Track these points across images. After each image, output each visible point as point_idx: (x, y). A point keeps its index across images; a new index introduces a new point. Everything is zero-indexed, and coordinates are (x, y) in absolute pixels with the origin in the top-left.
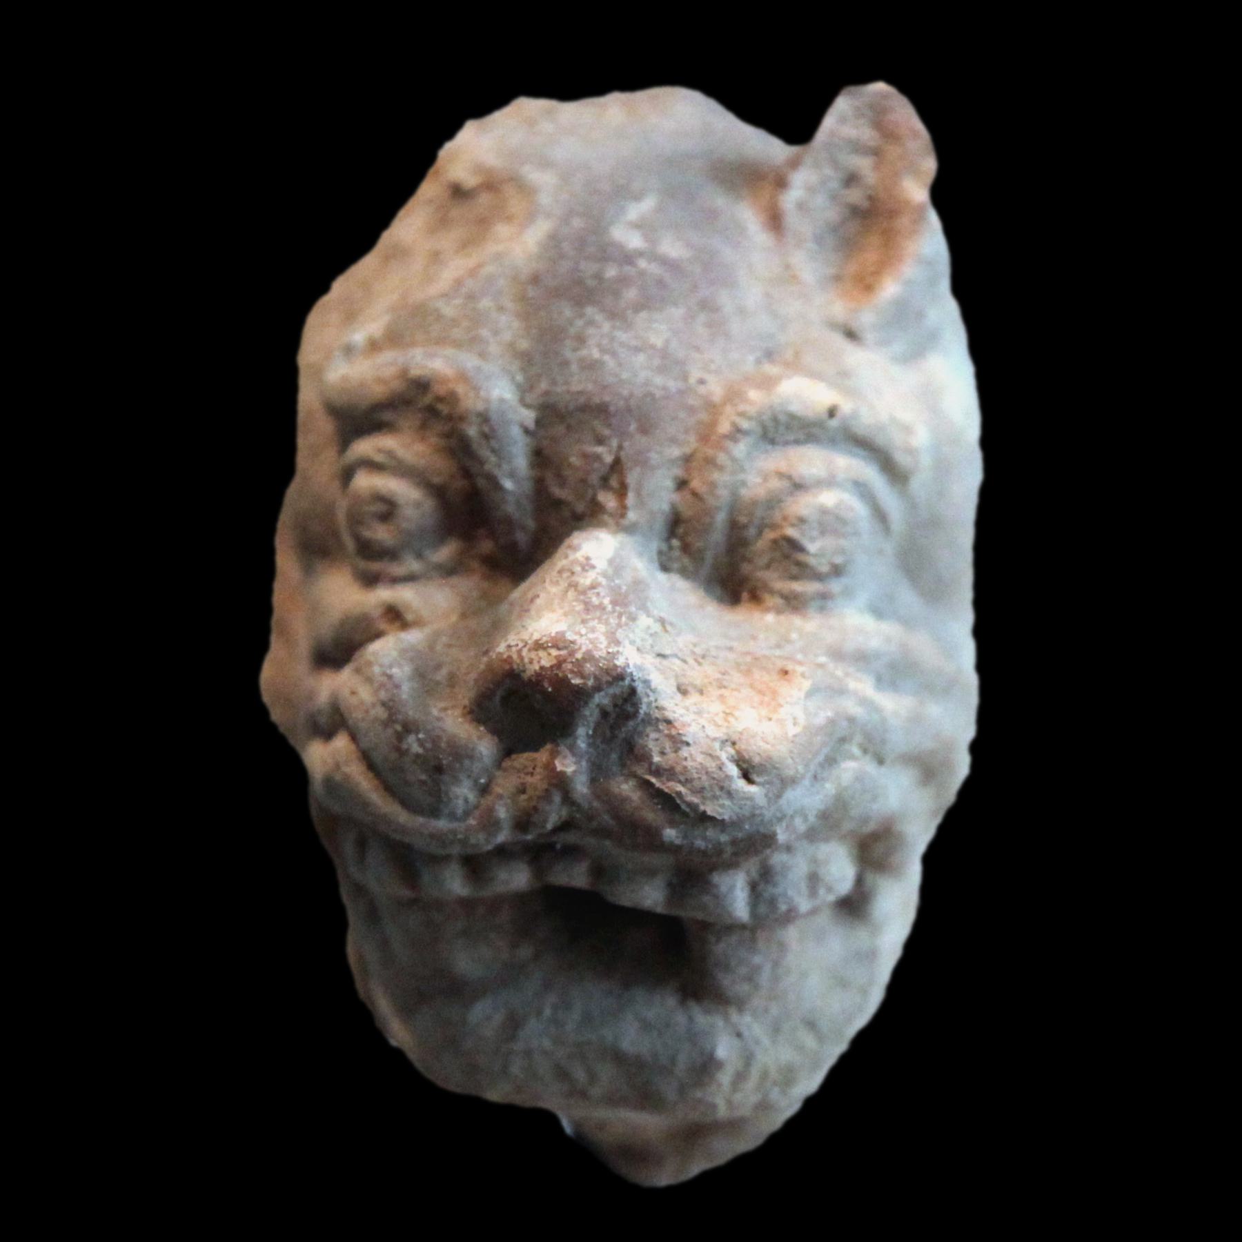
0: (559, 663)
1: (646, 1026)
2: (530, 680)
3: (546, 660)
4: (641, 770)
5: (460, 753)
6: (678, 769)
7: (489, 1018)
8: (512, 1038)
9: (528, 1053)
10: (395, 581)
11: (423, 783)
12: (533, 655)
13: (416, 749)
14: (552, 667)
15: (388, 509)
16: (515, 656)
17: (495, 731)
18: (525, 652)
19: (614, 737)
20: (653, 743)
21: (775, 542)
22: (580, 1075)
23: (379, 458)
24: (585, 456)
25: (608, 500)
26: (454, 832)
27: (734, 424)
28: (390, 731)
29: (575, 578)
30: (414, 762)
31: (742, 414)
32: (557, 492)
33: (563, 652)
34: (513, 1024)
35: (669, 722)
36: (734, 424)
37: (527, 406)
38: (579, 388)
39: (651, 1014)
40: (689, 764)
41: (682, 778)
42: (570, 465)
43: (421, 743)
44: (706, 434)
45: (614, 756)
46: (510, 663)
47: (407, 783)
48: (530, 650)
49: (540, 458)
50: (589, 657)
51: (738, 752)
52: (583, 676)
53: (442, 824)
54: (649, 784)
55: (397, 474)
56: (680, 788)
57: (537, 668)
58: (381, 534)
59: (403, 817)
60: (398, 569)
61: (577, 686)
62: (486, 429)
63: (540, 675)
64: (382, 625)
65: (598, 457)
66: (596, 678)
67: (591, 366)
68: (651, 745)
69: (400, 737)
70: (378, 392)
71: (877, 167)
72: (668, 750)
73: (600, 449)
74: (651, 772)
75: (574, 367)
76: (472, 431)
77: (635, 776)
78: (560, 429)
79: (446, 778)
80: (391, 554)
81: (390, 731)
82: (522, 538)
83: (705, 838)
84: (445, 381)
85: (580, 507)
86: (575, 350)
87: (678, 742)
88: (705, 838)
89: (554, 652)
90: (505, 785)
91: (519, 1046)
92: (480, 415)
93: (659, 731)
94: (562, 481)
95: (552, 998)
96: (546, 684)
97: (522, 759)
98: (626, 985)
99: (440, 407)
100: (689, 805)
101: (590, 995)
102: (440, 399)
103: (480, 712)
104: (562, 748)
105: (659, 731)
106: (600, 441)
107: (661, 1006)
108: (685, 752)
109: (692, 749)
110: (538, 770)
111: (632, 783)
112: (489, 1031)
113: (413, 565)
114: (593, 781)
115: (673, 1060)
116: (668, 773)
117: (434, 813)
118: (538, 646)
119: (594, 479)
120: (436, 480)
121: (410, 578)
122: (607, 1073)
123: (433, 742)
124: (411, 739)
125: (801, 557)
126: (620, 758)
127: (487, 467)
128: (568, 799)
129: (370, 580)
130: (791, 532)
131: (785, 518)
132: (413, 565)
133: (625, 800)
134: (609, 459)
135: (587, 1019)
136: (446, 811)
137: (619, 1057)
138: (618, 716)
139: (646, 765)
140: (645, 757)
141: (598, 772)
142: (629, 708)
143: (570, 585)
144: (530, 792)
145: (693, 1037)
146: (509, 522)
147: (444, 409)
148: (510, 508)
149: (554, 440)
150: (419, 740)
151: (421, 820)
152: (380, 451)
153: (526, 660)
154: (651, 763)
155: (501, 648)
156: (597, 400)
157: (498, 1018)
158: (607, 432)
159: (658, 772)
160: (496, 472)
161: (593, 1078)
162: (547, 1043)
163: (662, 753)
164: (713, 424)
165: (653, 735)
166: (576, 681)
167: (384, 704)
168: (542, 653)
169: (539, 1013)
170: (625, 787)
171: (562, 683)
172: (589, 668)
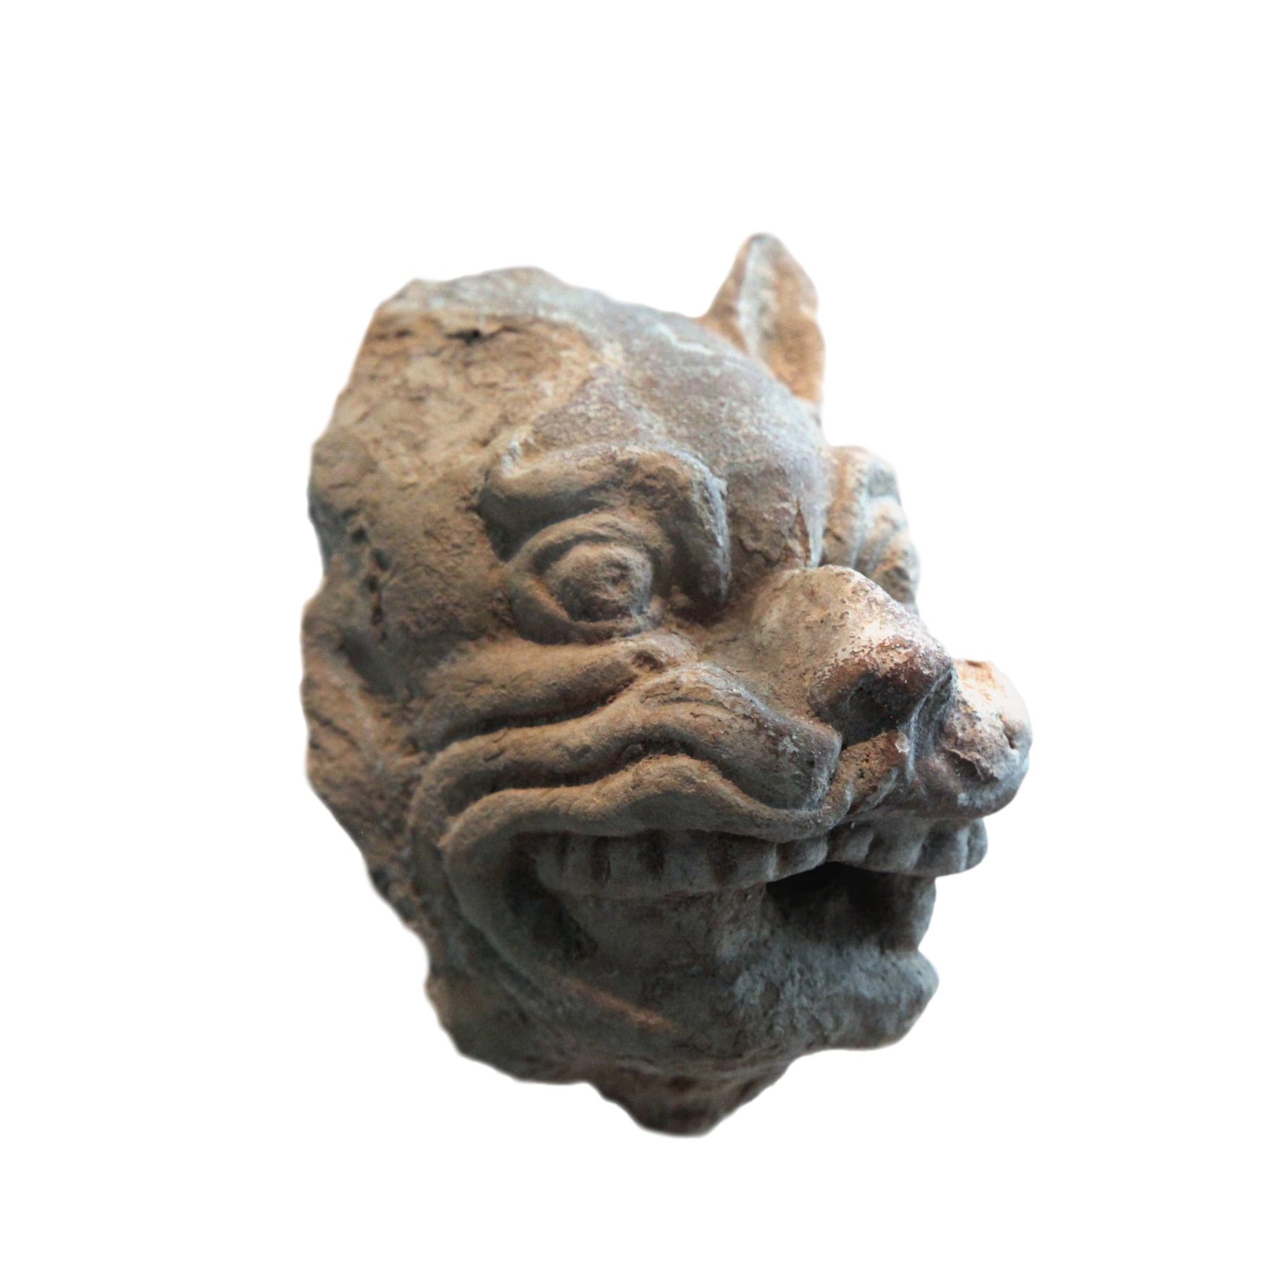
0: (911, 660)
1: (870, 974)
2: (885, 677)
3: (898, 658)
4: (947, 745)
5: (825, 749)
6: (977, 740)
7: (752, 990)
8: (777, 1000)
9: (791, 1012)
10: (625, 634)
11: (799, 777)
12: (883, 656)
13: (792, 748)
14: (905, 663)
15: (622, 572)
16: (867, 660)
17: (838, 728)
18: (874, 654)
19: (931, 719)
20: (956, 721)
21: (887, 573)
22: (829, 1023)
23: (602, 532)
24: (776, 511)
25: (798, 549)
26: (814, 818)
27: (858, 480)
28: (762, 738)
29: (870, 595)
30: (791, 760)
31: (860, 471)
32: (751, 544)
33: (910, 650)
34: (774, 991)
35: (964, 703)
36: (858, 480)
37: (720, 477)
38: (758, 457)
39: (870, 965)
40: (983, 735)
41: (979, 747)
42: (764, 520)
43: (795, 743)
44: (839, 488)
45: (930, 736)
46: (866, 666)
47: (782, 781)
48: (878, 653)
49: (735, 518)
50: (928, 653)
51: (1005, 723)
52: (930, 668)
53: (804, 812)
54: (955, 756)
55: (615, 544)
56: (978, 756)
57: (892, 665)
58: (614, 594)
59: (766, 811)
60: (625, 624)
61: (928, 676)
62: (707, 495)
63: (895, 672)
64: (635, 670)
65: (786, 512)
66: (938, 669)
67: (756, 440)
68: (956, 723)
69: (775, 741)
70: (590, 478)
71: (779, 299)
72: (968, 727)
73: (786, 505)
74: (956, 745)
75: (743, 441)
76: (696, 498)
77: (944, 751)
78: (746, 493)
79: (815, 770)
80: (623, 612)
81: (762, 738)
82: (724, 586)
83: (982, 798)
84: (654, 461)
85: (775, 554)
86: (735, 430)
87: (972, 718)
88: (982, 798)
89: (903, 651)
90: (849, 773)
91: (782, 1008)
92: (700, 483)
93: (959, 711)
94: (757, 535)
95: (796, 964)
96: (902, 678)
97: (859, 749)
98: (839, 947)
99: (649, 482)
100: (983, 770)
101: (820, 956)
102: (649, 476)
103: (825, 712)
104: (900, 733)
105: (959, 711)
106: (784, 498)
107: (868, 957)
108: (979, 726)
109: (983, 722)
110: (872, 755)
111: (942, 756)
112: (755, 1001)
113: (639, 620)
114: (917, 758)
115: (899, 999)
116: (971, 745)
117: (797, 804)
118: (883, 648)
119: (784, 529)
120: (653, 545)
121: (637, 631)
122: (848, 1018)
123: (806, 741)
124: (786, 741)
125: (904, 583)
126: (934, 737)
127: (707, 527)
128: (902, 776)
129: (603, 637)
130: (901, 564)
131: (894, 553)
132: (639, 620)
133: (937, 772)
134: (794, 512)
135: (829, 978)
136: (808, 800)
137: (858, 1003)
138: (936, 701)
139: (952, 741)
140: (951, 735)
141: (920, 749)
142: (944, 694)
143: (870, 602)
144: (868, 774)
145: (904, 977)
146: (716, 572)
147: (659, 485)
148: (718, 561)
149: (744, 502)
150: (792, 741)
151: (785, 812)
152: (602, 526)
153: (879, 661)
154: (957, 738)
155: (842, 656)
156: (775, 465)
157: (760, 987)
158: (787, 490)
159: (961, 744)
160: (715, 531)
161: (838, 1022)
162: (805, 1001)
163: (964, 729)
164: (841, 482)
165: (956, 715)
166: (926, 672)
167: (745, 717)
168: (892, 653)
169: (792, 977)
170: (937, 761)
171: (915, 675)
172: (932, 661)
